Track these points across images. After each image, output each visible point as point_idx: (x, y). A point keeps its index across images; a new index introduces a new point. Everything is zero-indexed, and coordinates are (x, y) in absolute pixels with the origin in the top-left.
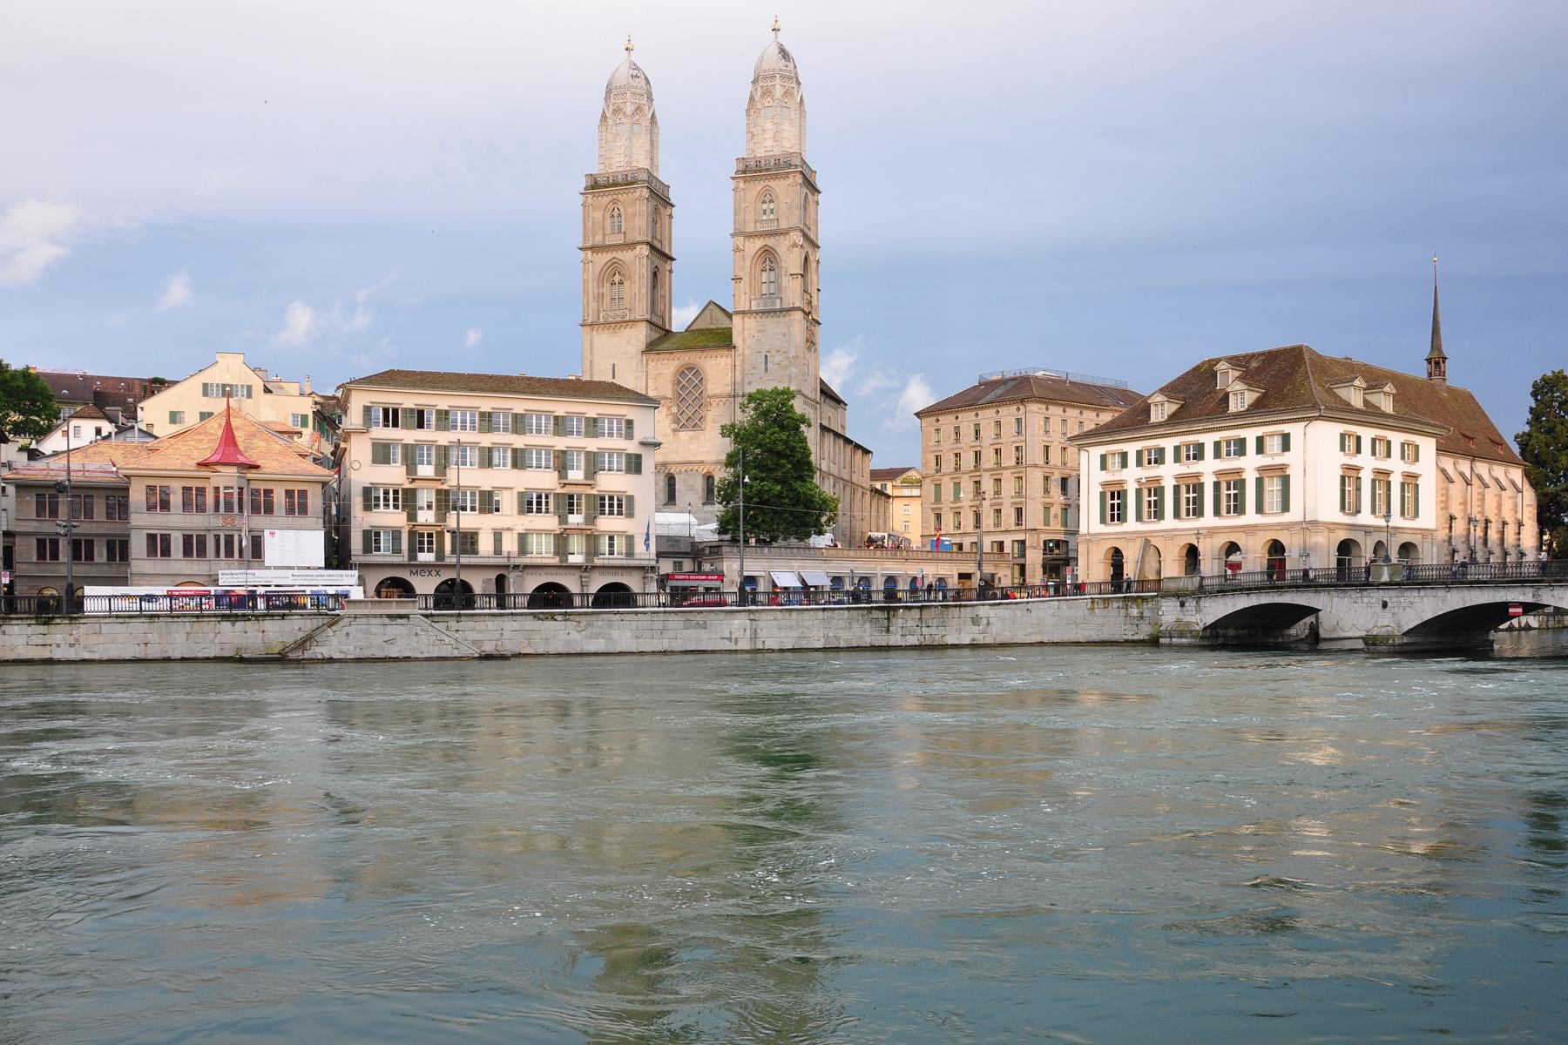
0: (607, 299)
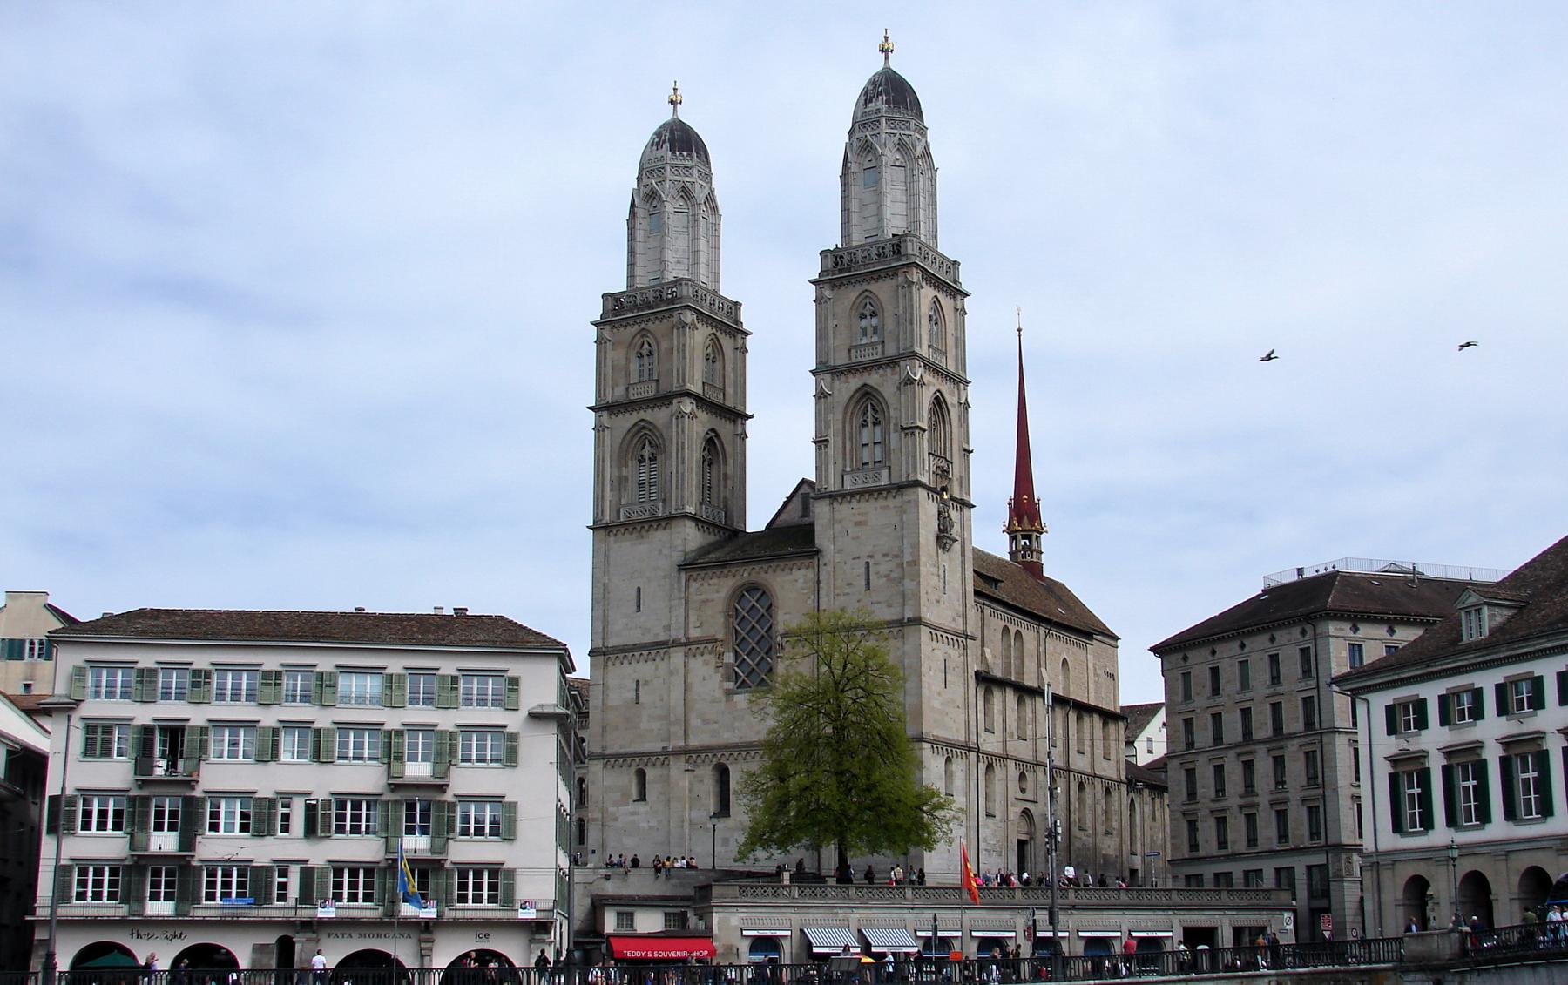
0: (632, 485)
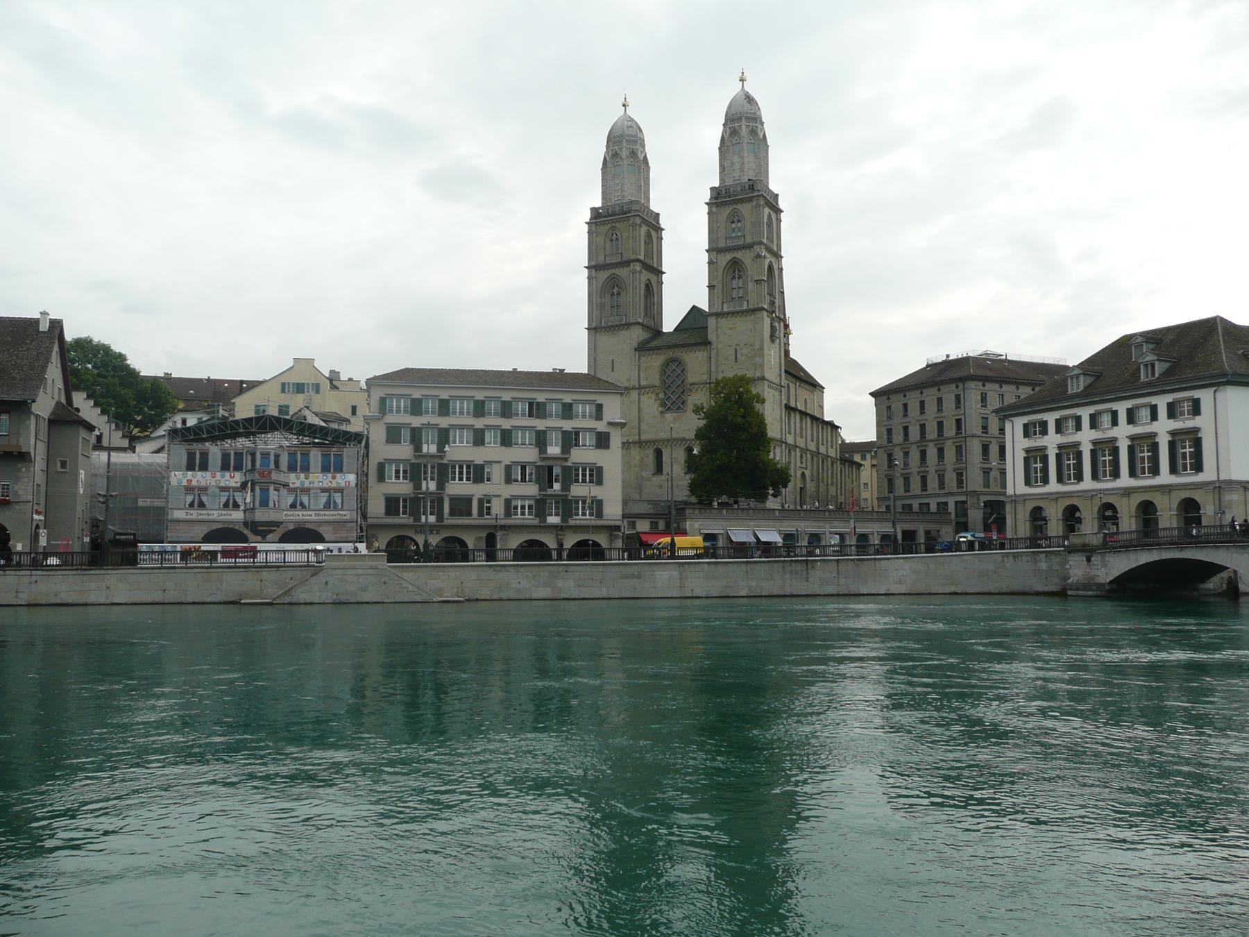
0: (608, 307)
